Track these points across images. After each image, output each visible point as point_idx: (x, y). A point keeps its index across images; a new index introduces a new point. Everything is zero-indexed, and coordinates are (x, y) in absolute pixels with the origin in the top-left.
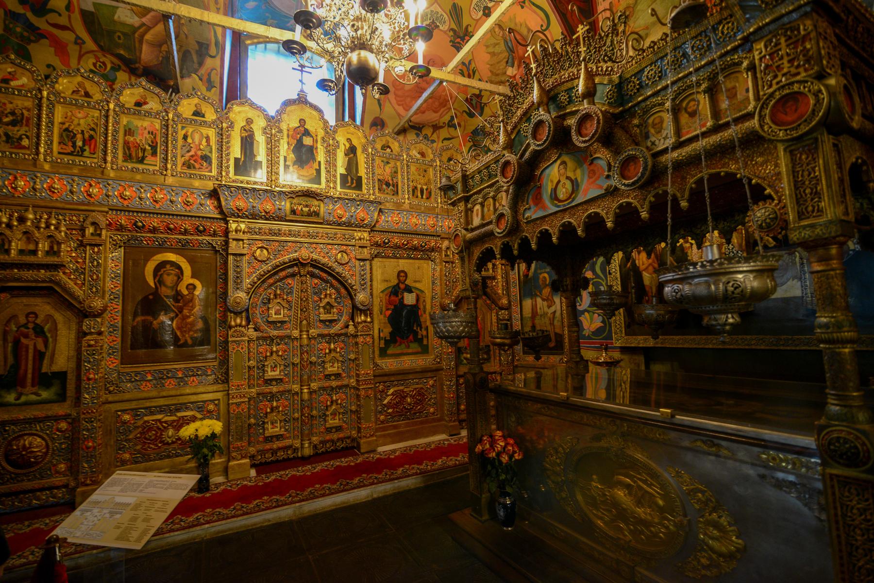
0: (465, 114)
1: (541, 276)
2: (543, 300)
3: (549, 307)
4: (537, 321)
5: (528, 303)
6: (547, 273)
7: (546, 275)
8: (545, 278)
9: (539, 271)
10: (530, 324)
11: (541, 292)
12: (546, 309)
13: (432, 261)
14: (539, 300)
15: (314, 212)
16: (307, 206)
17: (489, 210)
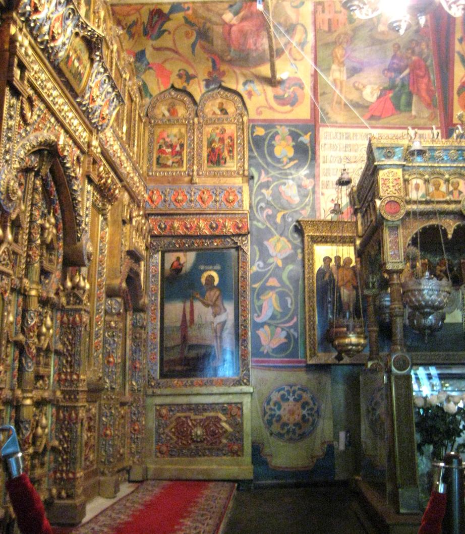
0: (142, 26)
1: (205, 275)
2: (207, 305)
3: (215, 315)
4: (192, 333)
5: (175, 309)
6: (216, 271)
7: (214, 274)
8: (211, 278)
9: (202, 267)
10: (178, 336)
11: (203, 295)
12: (210, 317)
13: (103, 215)
14: (198, 305)
15: (80, 74)
16: (79, 59)
17: (437, 189)
